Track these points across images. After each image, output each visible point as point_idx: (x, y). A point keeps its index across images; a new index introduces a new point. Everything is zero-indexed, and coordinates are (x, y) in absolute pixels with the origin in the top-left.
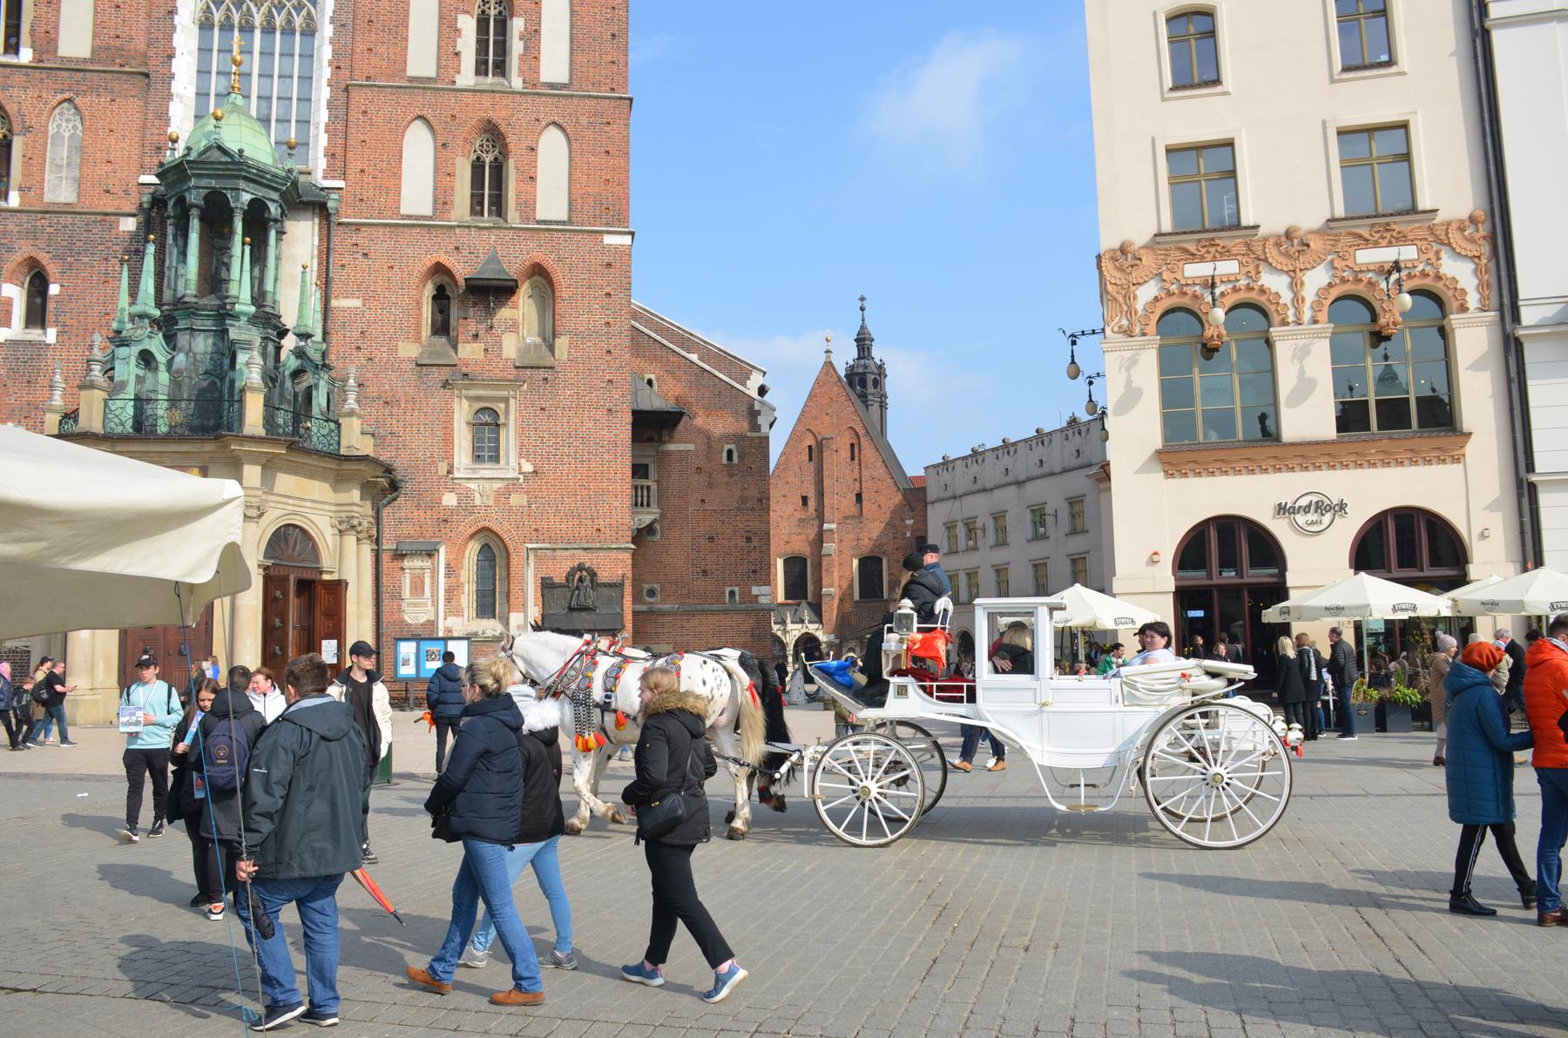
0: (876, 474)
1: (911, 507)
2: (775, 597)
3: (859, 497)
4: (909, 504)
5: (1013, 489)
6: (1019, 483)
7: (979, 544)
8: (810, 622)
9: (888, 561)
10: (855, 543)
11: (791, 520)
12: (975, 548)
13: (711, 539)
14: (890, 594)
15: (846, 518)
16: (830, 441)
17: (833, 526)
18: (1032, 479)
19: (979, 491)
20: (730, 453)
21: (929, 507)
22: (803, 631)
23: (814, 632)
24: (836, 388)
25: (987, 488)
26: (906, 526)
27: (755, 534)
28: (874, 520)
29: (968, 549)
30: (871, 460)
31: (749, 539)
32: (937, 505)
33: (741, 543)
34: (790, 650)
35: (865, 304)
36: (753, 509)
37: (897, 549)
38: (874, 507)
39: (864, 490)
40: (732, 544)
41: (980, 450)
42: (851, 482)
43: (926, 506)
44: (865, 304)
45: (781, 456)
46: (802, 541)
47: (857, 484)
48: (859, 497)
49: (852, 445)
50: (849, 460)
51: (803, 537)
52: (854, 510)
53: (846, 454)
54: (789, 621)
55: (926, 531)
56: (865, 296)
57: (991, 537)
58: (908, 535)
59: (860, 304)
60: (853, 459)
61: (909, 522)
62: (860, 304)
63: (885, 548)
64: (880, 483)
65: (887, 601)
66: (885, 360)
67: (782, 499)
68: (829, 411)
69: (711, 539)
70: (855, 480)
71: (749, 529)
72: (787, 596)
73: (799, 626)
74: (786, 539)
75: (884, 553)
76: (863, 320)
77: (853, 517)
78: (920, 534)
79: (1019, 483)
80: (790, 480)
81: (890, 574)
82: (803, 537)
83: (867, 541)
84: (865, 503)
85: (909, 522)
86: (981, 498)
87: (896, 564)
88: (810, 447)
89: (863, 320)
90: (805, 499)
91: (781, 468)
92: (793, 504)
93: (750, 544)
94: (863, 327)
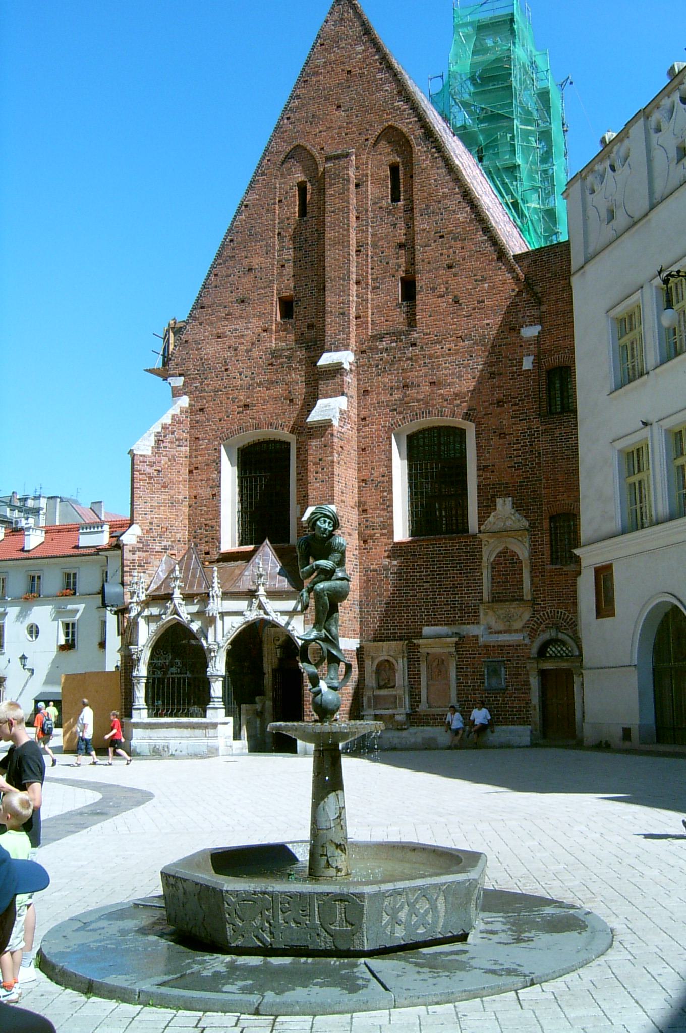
2: (216, 540)
8: (273, 595)
10: (397, 396)
11: (255, 353)
14: (481, 520)
17: (346, 358)
21: (575, 281)
22: (252, 615)
23: (282, 620)
26: (522, 343)
34: (218, 666)
37: (500, 403)
38: (444, 304)
39: (419, 267)
45: (239, 212)
49: (394, 169)
50: (387, 202)
51: (279, 390)
52: (399, 317)
54: (217, 590)
58: (527, 363)
60: (395, 199)
61: (530, 332)
65: (474, 536)
67: (236, 309)
68: (345, 99)
73: (241, 605)
77: (396, 335)
78: (554, 360)
80: (256, 262)
81: (482, 468)
82: (279, 390)
85: (530, 332)
87: (495, 441)
91: (238, 239)
92: (259, 317)
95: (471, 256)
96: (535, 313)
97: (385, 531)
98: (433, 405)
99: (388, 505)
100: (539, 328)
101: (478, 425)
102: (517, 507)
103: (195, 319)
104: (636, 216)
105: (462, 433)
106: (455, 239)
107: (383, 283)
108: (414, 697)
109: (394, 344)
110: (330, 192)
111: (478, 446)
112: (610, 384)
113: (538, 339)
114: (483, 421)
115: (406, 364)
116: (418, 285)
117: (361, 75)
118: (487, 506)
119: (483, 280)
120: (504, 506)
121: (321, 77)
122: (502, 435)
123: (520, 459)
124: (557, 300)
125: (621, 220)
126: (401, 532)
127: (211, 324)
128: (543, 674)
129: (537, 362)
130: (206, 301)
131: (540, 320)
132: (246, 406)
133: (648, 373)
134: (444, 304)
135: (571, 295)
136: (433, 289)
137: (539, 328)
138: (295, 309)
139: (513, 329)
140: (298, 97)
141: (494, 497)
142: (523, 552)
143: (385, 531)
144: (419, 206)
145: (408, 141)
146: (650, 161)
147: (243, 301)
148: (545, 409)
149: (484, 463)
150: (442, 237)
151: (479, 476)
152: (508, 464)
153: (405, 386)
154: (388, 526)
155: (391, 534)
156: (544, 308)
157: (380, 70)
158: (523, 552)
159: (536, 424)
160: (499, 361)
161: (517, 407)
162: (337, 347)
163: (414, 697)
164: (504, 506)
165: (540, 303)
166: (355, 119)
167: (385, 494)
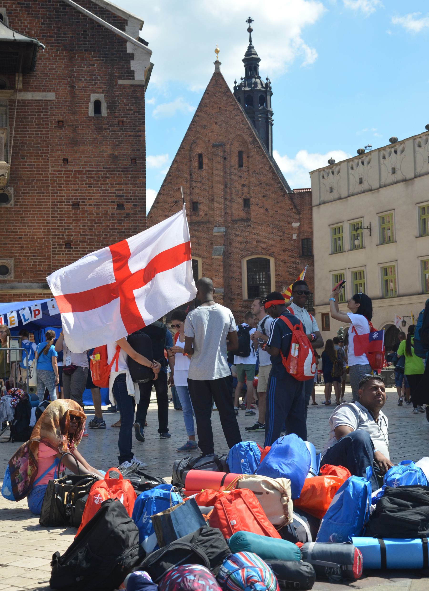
1: (297, 210)
4: (295, 207)
5: (401, 186)
6: (405, 180)
7: (366, 243)
9: (276, 262)
10: (244, 245)
12: (362, 247)
13: (76, 205)
15: (235, 221)
16: (220, 150)
18: (421, 176)
19: (364, 192)
20: (97, 104)
21: (315, 210)
24: (225, 98)
25: (373, 187)
26: (293, 229)
27: (128, 199)
28: (262, 224)
29: (354, 248)
31: (120, 206)
32: (322, 206)
33: (112, 209)
35: (253, 25)
36: (125, 170)
37: (284, 251)
38: (262, 211)
40: (101, 210)
41: (367, 151)
42: (239, 188)
43: (311, 209)
44: (253, 25)
45: (173, 164)
47: (246, 190)
49: (240, 153)
52: (242, 214)
53: (234, 161)
55: (312, 233)
56: (252, 18)
57: (376, 237)
58: (295, 237)
59: (247, 25)
60: (241, 165)
61: (296, 225)
62: (247, 25)
63: (272, 250)
64: (267, 188)
66: (271, 80)
68: (219, 120)
69: (76, 205)
70: (244, 185)
71: (120, 193)
75: (271, 255)
76: (251, 41)
77: (242, 220)
79: (405, 180)
81: (277, 275)
83: (255, 243)
84: (253, 208)
85: (296, 225)
86: (367, 197)
87: (282, 265)
89: (251, 41)
91: (173, 175)
93: (122, 211)
94: (250, 48)
95: (272, 193)
96: (298, 217)
97: (239, 297)
98: (258, 250)
99: (240, 287)
100: (299, 224)
101: (276, 258)
103: (155, 208)
104: (342, 196)
105: (269, 261)
106: (266, 185)
107: (236, 200)
109: (241, 225)
111: (276, 267)
112: (330, 251)
113: (299, 228)
114: (277, 257)
116: (251, 202)
119: (277, 203)
121: (208, 109)
122: (285, 263)
123: (291, 272)
124: (306, 213)
125: (335, 195)
127: (162, 211)
129: (298, 237)
130: (160, 201)
131: (299, 220)
133: (345, 252)
135: (312, 212)
136: (258, 205)
137: (299, 224)
138: (199, 207)
139: (289, 223)
140: (198, 116)
141: (282, 285)
143: (239, 297)
145: (246, 142)
146: (348, 178)
148: (301, 254)
149: (278, 273)
150: (261, 184)
151: (276, 278)
152: (288, 274)
153: (247, 242)
154: (241, 294)
155: (242, 298)
156: (301, 216)
159: (298, 260)
160: (283, 235)
161: (290, 253)
162: (220, 225)
165: (299, 213)
167: (239, 283)
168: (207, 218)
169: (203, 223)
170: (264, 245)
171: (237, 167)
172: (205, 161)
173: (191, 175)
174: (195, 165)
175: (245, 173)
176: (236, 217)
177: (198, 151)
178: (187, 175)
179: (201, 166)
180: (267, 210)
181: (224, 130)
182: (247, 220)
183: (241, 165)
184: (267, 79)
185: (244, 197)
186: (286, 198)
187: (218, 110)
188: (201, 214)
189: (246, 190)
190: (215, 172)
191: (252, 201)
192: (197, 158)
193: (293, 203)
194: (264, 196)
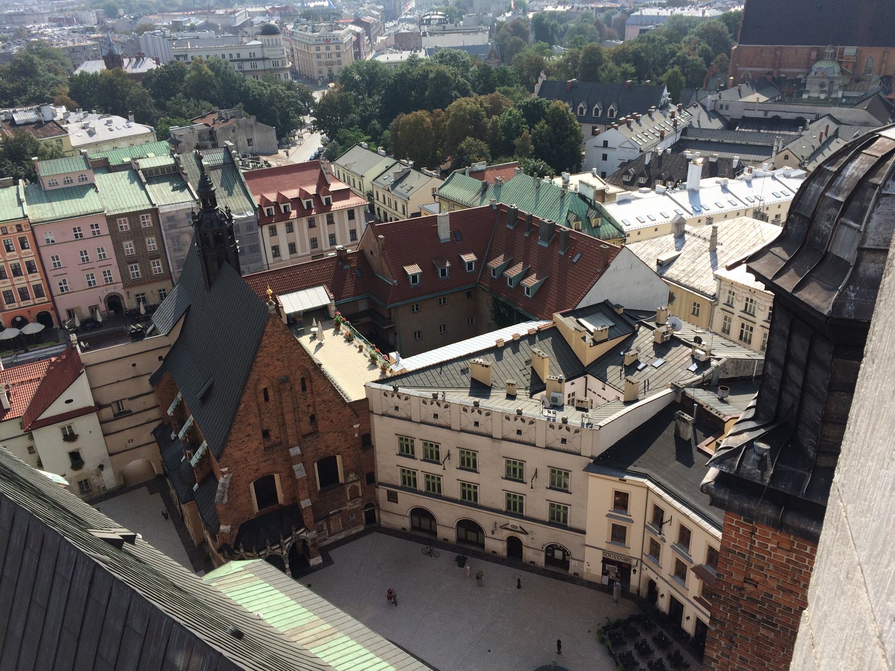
0: (326, 398)
3: (313, 418)
4: (355, 413)
10: (315, 453)
15: (305, 436)
30: (321, 389)
46: (269, 465)
47: (311, 409)
48: (313, 418)
49: (303, 380)
53: (298, 388)
58: (356, 435)
60: (304, 389)
61: (356, 426)
63: (339, 450)
64: (330, 404)
70: (309, 406)
72: (260, 507)
74: (255, 468)
77: (311, 434)
78: (365, 432)
80: (251, 422)
81: (344, 466)
82: (270, 462)
83: (324, 448)
85: (356, 426)
88: (265, 390)
90: (266, 434)
92: (257, 439)
102: (356, 474)
108: (329, 530)
110: (283, 395)
115: (316, 443)
117: (286, 347)
118: (346, 475)
120: (352, 476)
126: (319, 488)
128: (366, 513)
131: (359, 422)
132: (257, 470)
134: (327, 423)
142: (359, 484)
144: (315, 393)
147: (248, 436)
153: (317, 450)
157: (294, 345)
158: (359, 484)
163: (329, 530)
164: (352, 476)
165: (358, 416)
166: (286, 365)
168: (278, 440)
169: (276, 445)
170: (332, 448)
171: (301, 392)
172: (271, 393)
173: (259, 410)
174: (262, 399)
175: (309, 396)
176: (305, 432)
177: (263, 386)
178: (256, 411)
179: (267, 399)
180: (331, 421)
181: (286, 365)
182: (315, 433)
183: (304, 389)
184: (226, 207)
185: (310, 415)
186: (347, 407)
187: (278, 348)
188: (273, 438)
189: (311, 409)
190: (284, 405)
191: (317, 417)
192: (262, 394)
193: (353, 410)
194: (328, 411)
